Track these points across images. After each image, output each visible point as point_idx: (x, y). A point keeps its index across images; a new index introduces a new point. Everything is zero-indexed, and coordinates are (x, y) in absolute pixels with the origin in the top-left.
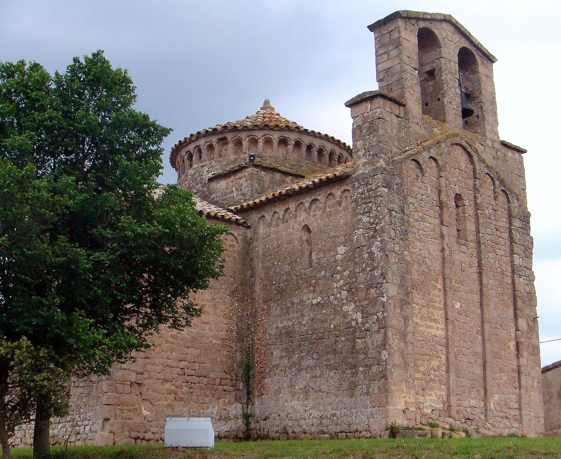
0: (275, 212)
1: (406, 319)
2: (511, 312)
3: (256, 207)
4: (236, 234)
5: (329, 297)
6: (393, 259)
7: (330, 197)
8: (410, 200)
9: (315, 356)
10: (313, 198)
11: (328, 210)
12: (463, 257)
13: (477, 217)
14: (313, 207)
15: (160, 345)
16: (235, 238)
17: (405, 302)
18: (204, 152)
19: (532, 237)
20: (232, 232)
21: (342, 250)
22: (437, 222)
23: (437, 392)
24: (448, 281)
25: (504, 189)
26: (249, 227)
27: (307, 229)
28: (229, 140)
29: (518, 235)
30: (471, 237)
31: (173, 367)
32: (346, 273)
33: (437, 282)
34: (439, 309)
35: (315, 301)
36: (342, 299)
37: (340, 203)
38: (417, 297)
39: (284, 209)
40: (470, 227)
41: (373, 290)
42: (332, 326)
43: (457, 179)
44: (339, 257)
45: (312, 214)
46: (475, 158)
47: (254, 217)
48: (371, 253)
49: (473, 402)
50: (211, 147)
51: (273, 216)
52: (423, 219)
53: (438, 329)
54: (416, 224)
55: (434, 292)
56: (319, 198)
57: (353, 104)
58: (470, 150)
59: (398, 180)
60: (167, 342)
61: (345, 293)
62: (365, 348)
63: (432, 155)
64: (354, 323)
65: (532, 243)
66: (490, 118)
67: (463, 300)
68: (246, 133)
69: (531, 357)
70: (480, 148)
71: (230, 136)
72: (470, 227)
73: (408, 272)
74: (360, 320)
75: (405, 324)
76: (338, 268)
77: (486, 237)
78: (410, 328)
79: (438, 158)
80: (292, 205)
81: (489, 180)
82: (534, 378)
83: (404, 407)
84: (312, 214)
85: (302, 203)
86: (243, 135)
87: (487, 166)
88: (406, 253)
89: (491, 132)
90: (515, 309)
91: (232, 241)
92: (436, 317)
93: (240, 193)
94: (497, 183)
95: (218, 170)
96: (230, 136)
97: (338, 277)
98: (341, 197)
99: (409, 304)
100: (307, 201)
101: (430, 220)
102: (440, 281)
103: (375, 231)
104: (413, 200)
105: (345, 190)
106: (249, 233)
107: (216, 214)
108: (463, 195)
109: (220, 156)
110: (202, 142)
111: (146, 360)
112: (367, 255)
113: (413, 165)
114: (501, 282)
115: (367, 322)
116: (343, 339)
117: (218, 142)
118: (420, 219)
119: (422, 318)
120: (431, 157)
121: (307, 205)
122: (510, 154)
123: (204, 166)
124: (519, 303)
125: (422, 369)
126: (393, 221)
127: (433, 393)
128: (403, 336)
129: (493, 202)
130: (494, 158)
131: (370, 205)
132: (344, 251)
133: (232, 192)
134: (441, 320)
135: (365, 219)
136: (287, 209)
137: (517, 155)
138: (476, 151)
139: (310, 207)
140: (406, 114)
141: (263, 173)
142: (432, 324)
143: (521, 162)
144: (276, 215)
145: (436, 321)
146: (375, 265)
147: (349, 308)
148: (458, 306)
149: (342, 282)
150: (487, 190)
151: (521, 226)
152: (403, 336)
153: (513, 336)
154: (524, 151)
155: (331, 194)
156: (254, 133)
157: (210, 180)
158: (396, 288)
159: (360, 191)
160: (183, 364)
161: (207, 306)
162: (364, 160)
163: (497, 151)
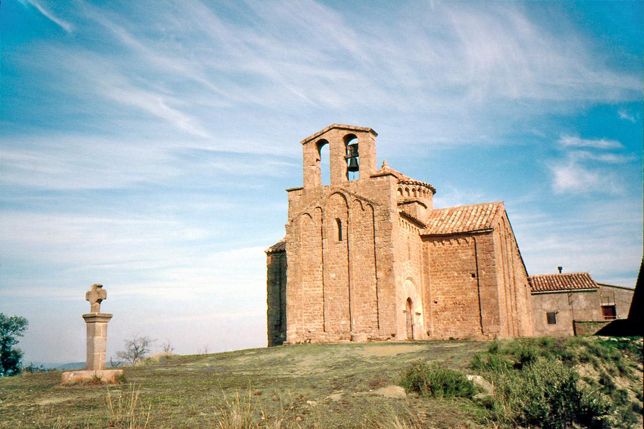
2: (374, 269)
23: (319, 321)
49: (343, 322)
52: (312, 240)
53: (319, 290)
55: (318, 273)
72: (344, 232)
83: (295, 330)
92: (318, 285)
94: (363, 202)
101: (316, 238)
120: (317, 208)
134: (322, 285)
142: (316, 288)
145: (318, 287)
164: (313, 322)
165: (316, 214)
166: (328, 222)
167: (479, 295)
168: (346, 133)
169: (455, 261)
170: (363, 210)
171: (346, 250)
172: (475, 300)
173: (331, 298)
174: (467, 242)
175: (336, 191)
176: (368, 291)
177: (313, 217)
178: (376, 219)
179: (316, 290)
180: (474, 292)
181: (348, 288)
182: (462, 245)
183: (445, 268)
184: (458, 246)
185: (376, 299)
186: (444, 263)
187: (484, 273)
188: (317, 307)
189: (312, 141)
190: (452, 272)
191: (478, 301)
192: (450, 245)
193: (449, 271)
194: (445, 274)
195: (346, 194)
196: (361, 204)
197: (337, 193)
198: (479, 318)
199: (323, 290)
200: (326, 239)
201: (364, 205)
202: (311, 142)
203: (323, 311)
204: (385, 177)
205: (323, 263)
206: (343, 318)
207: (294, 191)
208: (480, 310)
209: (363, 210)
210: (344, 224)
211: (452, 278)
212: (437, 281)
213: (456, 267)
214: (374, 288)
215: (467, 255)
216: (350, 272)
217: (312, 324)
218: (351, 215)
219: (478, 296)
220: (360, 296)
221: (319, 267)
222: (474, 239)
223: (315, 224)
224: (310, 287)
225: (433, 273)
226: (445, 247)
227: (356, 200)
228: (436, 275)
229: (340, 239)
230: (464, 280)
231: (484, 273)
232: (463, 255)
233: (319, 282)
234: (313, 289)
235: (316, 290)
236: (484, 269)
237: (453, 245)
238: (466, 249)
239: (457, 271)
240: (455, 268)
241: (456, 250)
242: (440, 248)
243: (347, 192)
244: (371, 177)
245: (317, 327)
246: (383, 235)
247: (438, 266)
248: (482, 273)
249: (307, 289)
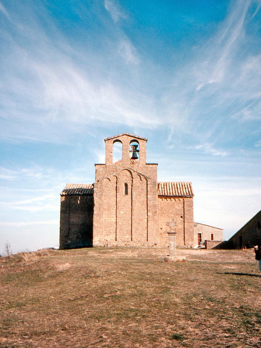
23: (113, 235)
34: (115, 214)
49: (127, 237)
55: (113, 210)
59: (99, 185)
72: (129, 191)
83: (99, 240)
90: (147, 210)
92: (113, 217)
94: (141, 176)
101: (113, 192)
127: (111, 235)
140: (106, 167)
142: (112, 218)
160: (80, 230)
164: (109, 236)
165: (113, 179)
166: (120, 184)
167: (184, 227)
168: (132, 139)
169: (173, 209)
170: (141, 180)
171: (130, 200)
172: (182, 229)
173: (120, 224)
174: (179, 200)
175: (126, 169)
176: (142, 222)
177: (111, 181)
178: (148, 186)
180: (182, 225)
181: (131, 219)
182: (177, 202)
183: (167, 212)
184: (175, 202)
185: (147, 226)
186: (167, 210)
187: (187, 216)
188: (112, 228)
189: (112, 140)
190: (171, 214)
191: (183, 230)
192: (171, 201)
193: (169, 214)
194: (167, 215)
195: (132, 171)
196: (140, 177)
197: (127, 169)
198: (184, 237)
199: (116, 219)
200: (119, 193)
201: (142, 178)
202: (111, 140)
203: (115, 230)
204: (154, 165)
205: (117, 205)
206: (127, 235)
207: (99, 165)
208: (184, 234)
209: (141, 180)
210: (129, 187)
211: (171, 217)
212: (163, 218)
213: (173, 212)
214: (146, 220)
215: (179, 207)
216: (132, 211)
217: (109, 237)
218: (134, 182)
219: (183, 227)
220: (137, 224)
221: (114, 207)
222: (184, 199)
223: (113, 184)
224: (108, 217)
225: (161, 214)
226: (168, 202)
227: (138, 175)
228: (161, 215)
229: (126, 193)
230: (177, 219)
231: (187, 216)
232: (177, 206)
233: (113, 215)
234: (110, 218)
236: (187, 214)
237: (172, 201)
238: (179, 204)
239: (173, 214)
240: (172, 213)
241: (174, 204)
242: (166, 202)
243: (132, 170)
244: (146, 164)
245: (111, 239)
246: (152, 194)
247: (164, 211)
248: (186, 216)
249: (106, 218)
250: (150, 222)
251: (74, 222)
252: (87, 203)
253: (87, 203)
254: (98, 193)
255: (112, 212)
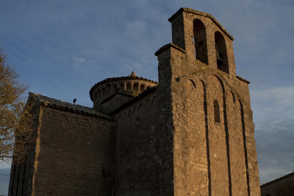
0: (125, 113)
1: (186, 162)
2: (244, 159)
3: (118, 111)
4: (108, 125)
5: (147, 152)
6: (177, 129)
7: (148, 101)
8: (188, 100)
9: (141, 183)
10: (141, 103)
11: (147, 108)
12: (217, 131)
13: (225, 111)
14: (141, 108)
15: (63, 179)
16: (108, 127)
17: (185, 153)
18: (101, 92)
19: (254, 123)
20: (106, 124)
21: (153, 127)
22: (203, 112)
24: (210, 143)
25: (239, 99)
26: (114, 122)
27: (138, 119)
28: (111, 85)
29: (247, 122)
30: (222, 121)
31: (71, 190)
32: (155, 139)
33: (204, 143)
35: (141, 155)
36: (153, 153)
37: (152, 104)
38: (192, 151)
39: (129, 110)
40: (222, 116)
41: (167, 147)
42: (148, 167)
43: (214, 92)
44: (152, 131)
45: (140, 111)
46: (224, 83)
47: (117, 116)
48: (166, 127)
50: (104, 89)
51: (124, 115)
54: (192, 113)
55: (202, 148)
56: (143, 103)
57: (157, 54)
58: (221, 78)
60: (67, 177)
61: (154, 150)
62: (163, 178)
63: (200, 79)
64: (158, 165)
65: (254, 126)
66: (232, 65)
67: (218, 153)
68: (118, 82)
69: (255, 182)
70: (227, 78)
71: (111, 83)
72: (222, 116)
73: (187, 137)
74: (161, 163)
75: (185, 165)
76: (152, 137)
77: (230, 121)
78: (188, 168)
79: (204, 81)
80: (132, 108)
81: (231, 94)
82: (257, 193)
84: (140, 111)
85: (136, 107)
86: (117, 82)
87: (230, 87)
88: (185, 127)
89: (232, 72)
91: (106, 128)
92: (203, 161)
93: (113, 107)
94: (235, 95)
95: (106, 98)
96: (111, 83)
97: (151, 141)
98: (153, 101)
99: (188, 154)
100: (138, 104)
102: (205, 143)
103: (168, 115)
104: (190, 101)
105: (155, 97)
106: (114, 124)
107: (96, 115)
108: (218, 101)
109: (108, 93)
110: (100, 87)
111: (55, 186)
112: (164, 128)
113: (190, 82)
114: (239, 144)
115: (164, 164)
116: (153, 174)
117: (107, 87)
118: (194, 110)
119: (195, 162)
121: (138, 107)
122: (242, 83)
123: (100, 98)
124: (248, 155)
125: (196, 189)
126: (178, 110)
128: (184, 171)
129: (234, 105)
130: (234, 84)
131: (166, 102)
132: (154, 128)
133: (110, 107)
134: (206, 163)
135: (164, 110)
136: (130, 111)
137: (245, 84)
138: (224, 79)
139: (139, 108)
141: (124, 98)
143: (247, 87)
144: (126, 114)
145: (203, 163)
146: (168, 133)
147: (156, 157)
148: (215, 156)
149: (153, 144)
150: (229, 99)
151: (248, 117)
152: (184, 171)
153: (246, 171)
154: (248, 83)
155: (148, 100)
156: (122, 81)
157: (102, 103)
158: (179, 146)
159: (161, 95)
161: (91, 159)
162: (163, 80)
163: (235, 81)
179: (201, 167)
181: (227, 171)
188: (203, 186)
214: (245, 176)
229: (217, 120)
234: (199, 165)
235: (201, 167)
250: (252, 181)
251: (66, 168)
252: (91, 133)
253: (91, 133)
254: (179, 106)
255: (200, 150)
